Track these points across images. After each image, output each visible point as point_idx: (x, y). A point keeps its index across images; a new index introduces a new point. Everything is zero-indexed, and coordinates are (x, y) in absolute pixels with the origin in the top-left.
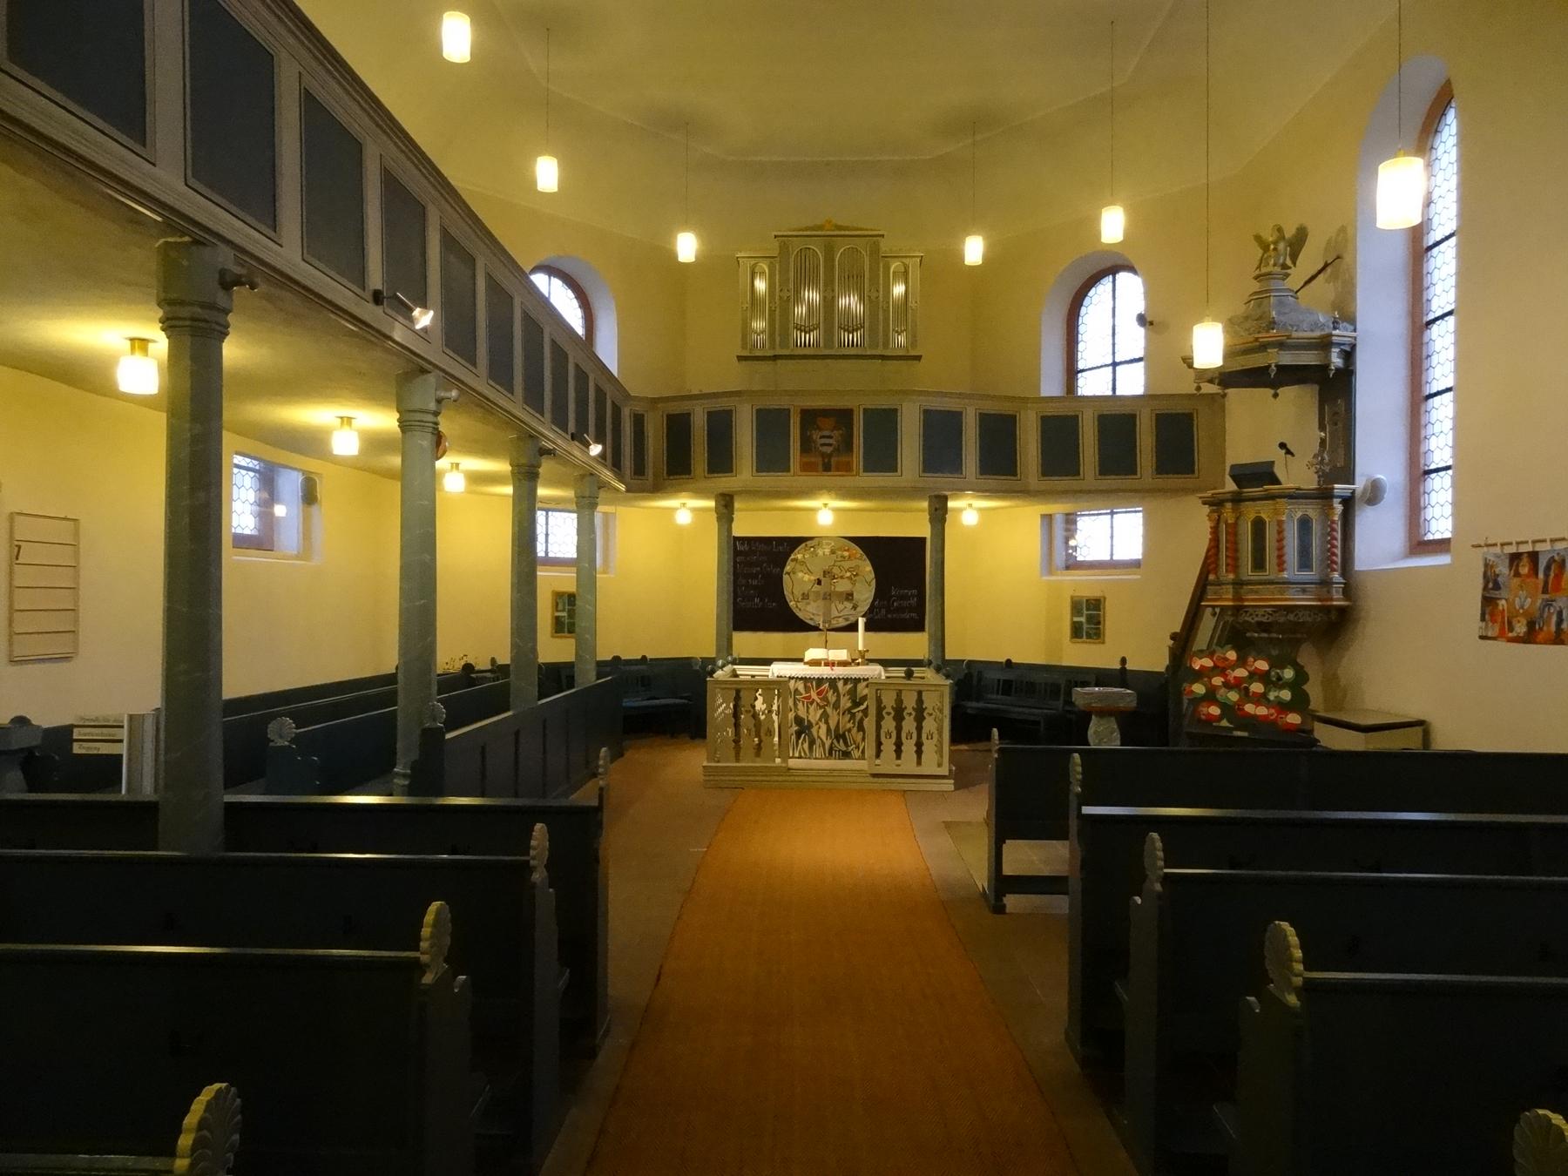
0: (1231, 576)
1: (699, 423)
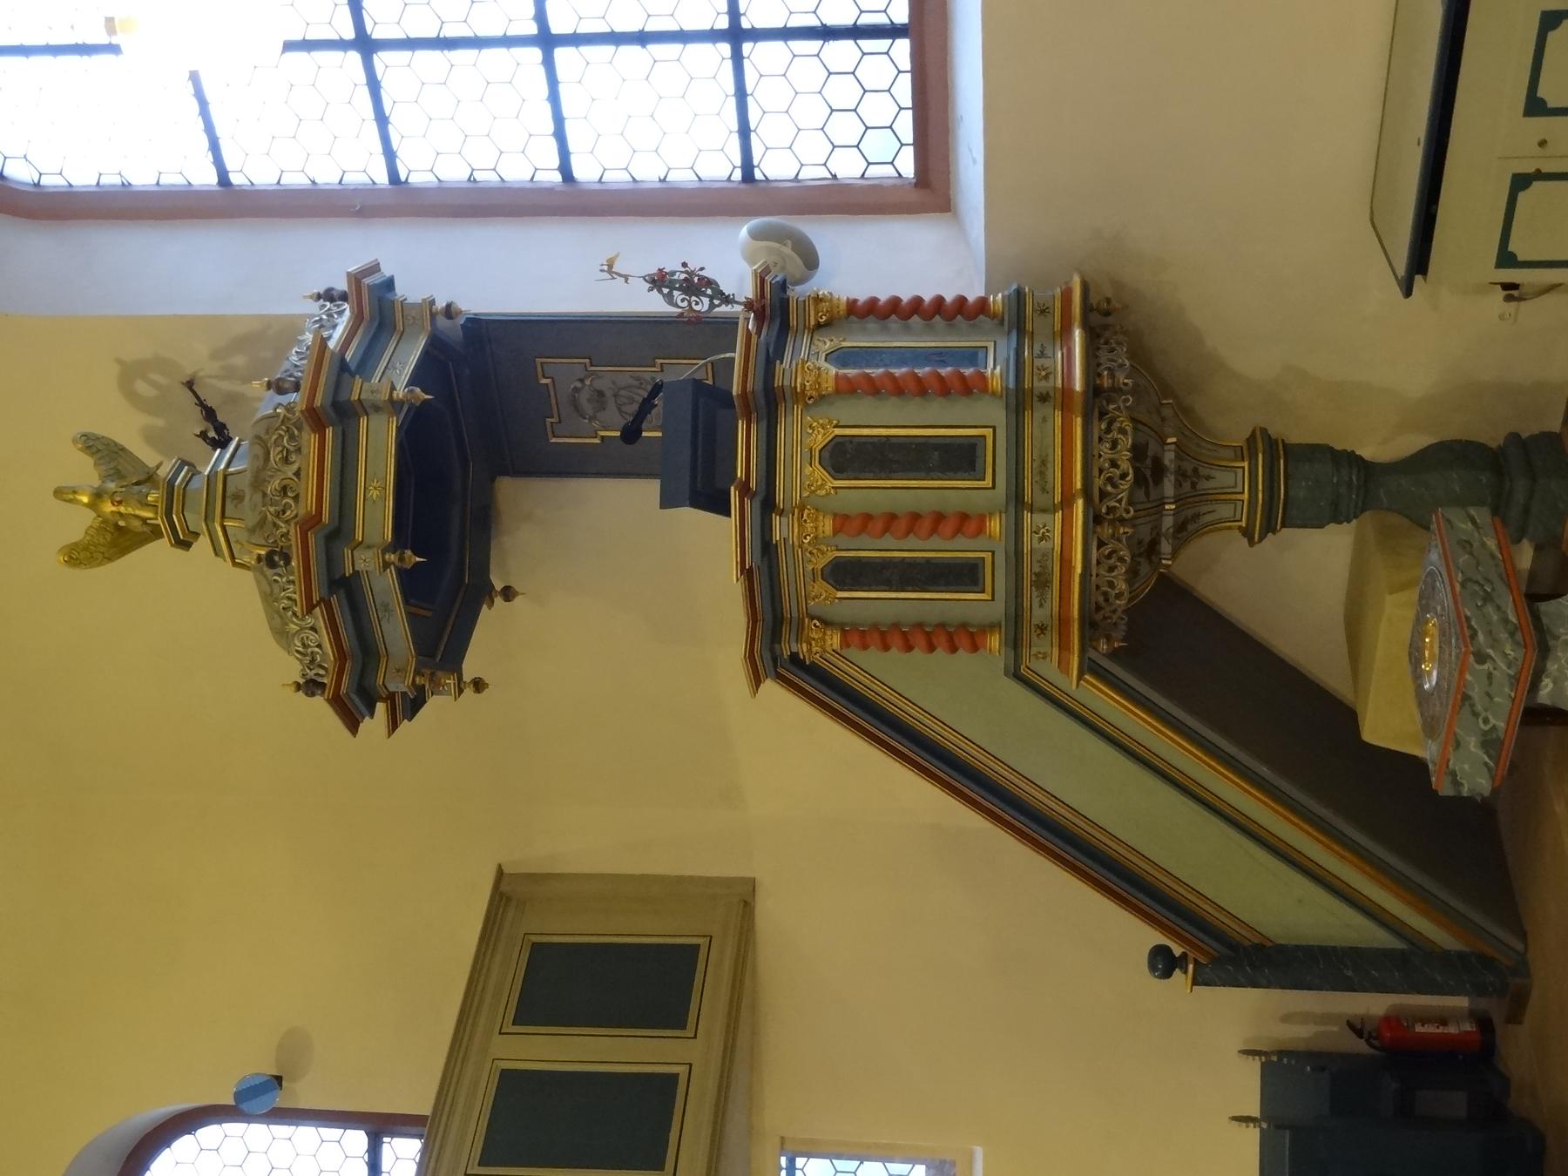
0: (995, 526)
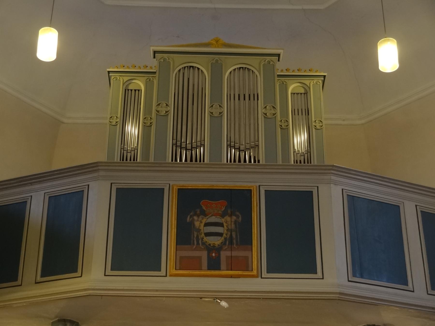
1: (37, 211)
